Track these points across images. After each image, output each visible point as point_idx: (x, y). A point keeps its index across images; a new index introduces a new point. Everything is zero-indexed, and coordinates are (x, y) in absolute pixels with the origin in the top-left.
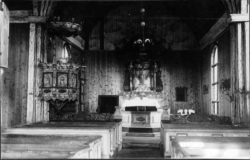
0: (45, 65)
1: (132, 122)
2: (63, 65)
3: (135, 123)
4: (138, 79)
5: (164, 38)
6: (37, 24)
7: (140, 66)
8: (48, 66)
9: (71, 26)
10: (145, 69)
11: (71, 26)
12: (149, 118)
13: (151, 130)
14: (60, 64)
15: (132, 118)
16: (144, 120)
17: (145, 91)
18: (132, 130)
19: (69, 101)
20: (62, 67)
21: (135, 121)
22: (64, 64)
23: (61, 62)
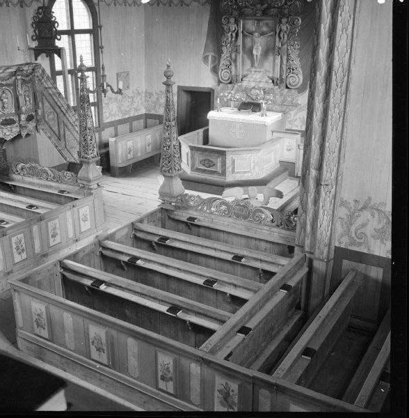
3: (198, 170)
4: (248, 58)
7: (251, 25)
10: (262, 34)
12: (224, 164)
15: (192, 157)
16: (214, 165)
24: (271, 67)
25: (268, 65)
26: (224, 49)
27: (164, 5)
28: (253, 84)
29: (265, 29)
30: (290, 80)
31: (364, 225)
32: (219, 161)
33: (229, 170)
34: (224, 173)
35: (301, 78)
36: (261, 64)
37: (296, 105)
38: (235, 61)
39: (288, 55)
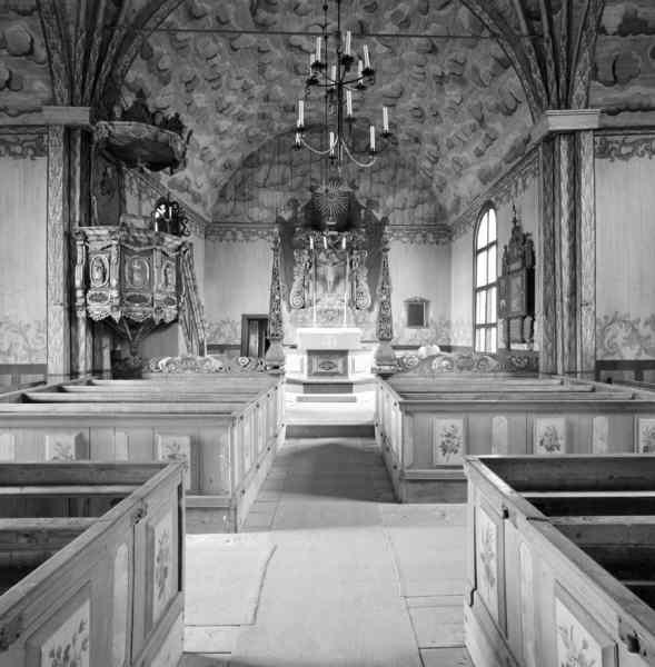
0: (91, 233)
1: (310, 371)
2: (136, 234)
3: (316, 374)
5: (376, 199)
6: (69, 131)
8: (99, 236)
9: (156, 136)
11: (156, 136)
12: (345, 364)
13: (348, 387)
14: (128, 231)
15: (310, 362)
17: (335, 307)
18: (308, 387)
19: (157, 323)
20: (134, 237)
21: (315, 369)
22: (138, 230)
23: (132, 224)
24: (344, 291)
25: (339, 289)
26: (296, 277)
27: (228, 241)
28: (326, 307)
29: (336, 260)
30: (360, 302)
31: (614, 337)
32: (339, 363)
33: (350, 374)
34: (345, 373)
35: (369, 297)
36: (334, 289)
37: (368, 322)
38: (308, 287)
39: (357, 281)
